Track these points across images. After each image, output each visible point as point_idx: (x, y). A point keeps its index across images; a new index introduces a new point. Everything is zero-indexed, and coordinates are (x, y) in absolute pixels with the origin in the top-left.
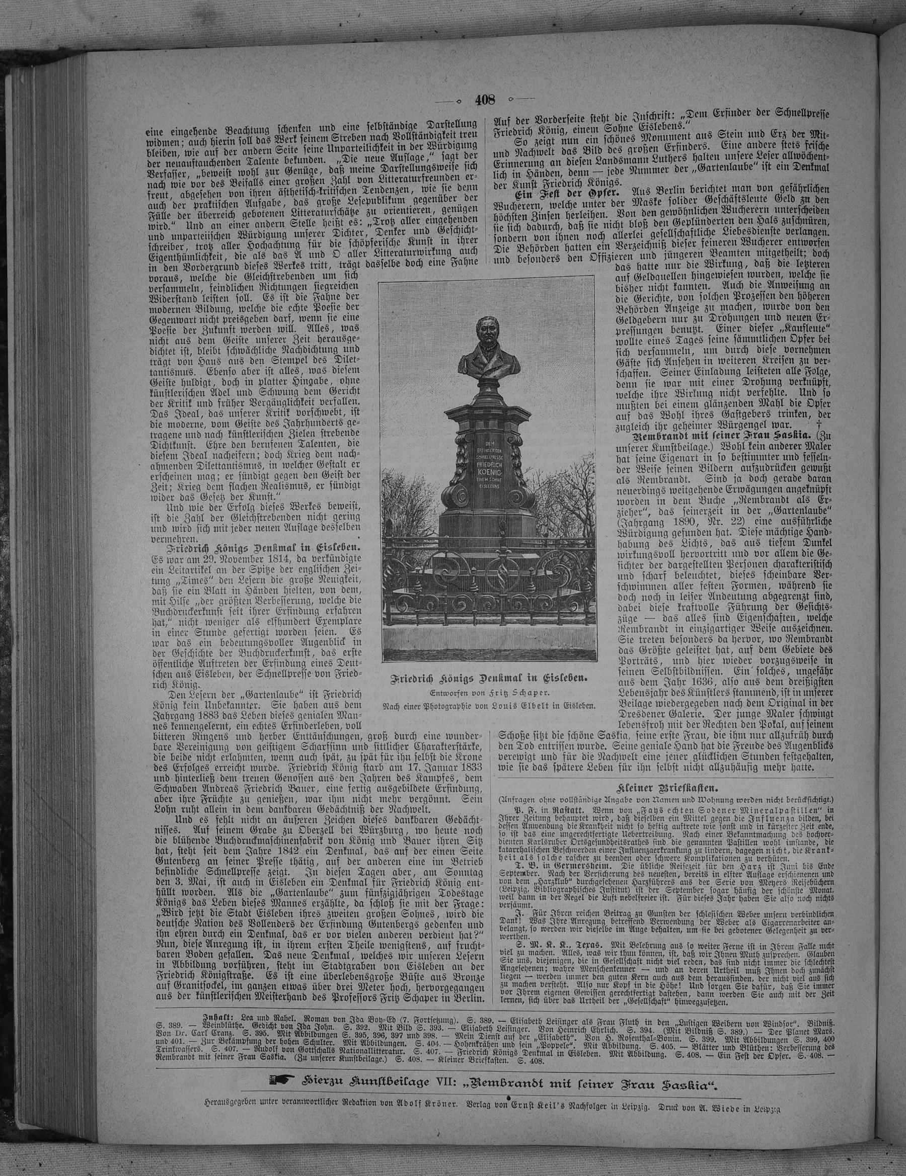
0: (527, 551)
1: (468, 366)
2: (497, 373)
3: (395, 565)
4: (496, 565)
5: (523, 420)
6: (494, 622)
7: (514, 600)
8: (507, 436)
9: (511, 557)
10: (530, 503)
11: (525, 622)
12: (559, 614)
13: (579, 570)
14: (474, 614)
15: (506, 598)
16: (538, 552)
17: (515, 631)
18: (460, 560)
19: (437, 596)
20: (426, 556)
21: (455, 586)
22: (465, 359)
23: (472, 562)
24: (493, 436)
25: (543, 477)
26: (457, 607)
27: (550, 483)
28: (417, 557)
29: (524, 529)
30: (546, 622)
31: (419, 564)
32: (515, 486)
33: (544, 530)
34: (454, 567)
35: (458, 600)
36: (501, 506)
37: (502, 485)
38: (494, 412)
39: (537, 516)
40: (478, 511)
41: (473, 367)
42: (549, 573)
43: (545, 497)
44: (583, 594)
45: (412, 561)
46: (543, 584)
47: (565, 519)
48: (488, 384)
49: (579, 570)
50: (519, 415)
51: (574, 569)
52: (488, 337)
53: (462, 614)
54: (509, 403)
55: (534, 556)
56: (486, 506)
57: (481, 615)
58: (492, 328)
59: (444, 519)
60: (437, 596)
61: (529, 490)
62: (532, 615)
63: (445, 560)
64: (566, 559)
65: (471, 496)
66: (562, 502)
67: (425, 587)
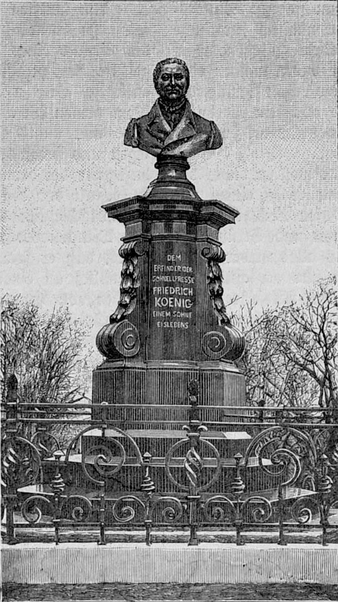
0: (231, 428)
1: (140, 134)
2: (185, 147)
3: (21, 447)
4: (183, 449)
5: (225, 222)
6: (179, 540)
7: (211, 505)
8: (200, 246)
9: (207, 437)
10: (237, 352)
11: (229, 540)
12: (282, 527)
13: (313, 459)
14: (147, 527)
15: (198, 502)
16: (248, 430)
17: (212, 554)
18: (124, 440)
19: (89, 498)
20: (72, 433)
21: (117, 481)
22: (135, 124)
23: (145, 444)
24: (178, 245)
25: (258, 313)
26: (121, 515)
27: (268, 321)
28: (56, 435)
29: (227, 393)
30: (261, 541)
31: (59, 447)
32: (213, 324)
33: (258, 395)
34: (116, 452)
35: (122, 504)
36: (190, 357)
37: (193, 323)
38: (180, 207)
39: (248, 373)
40: (155, 364)
41: (147, 138)
42: (266, 462)
43: (261, 343)
44: (320, 497)
45: (48, 442)
46: (256, 480)
47: (291, 379)
48: (171, 164)
49: (313, 459)
50: (219, 215)
51: (305, 457)
52: (172, 92)
53: (128, 526)
54: (205, 194)
55: (243, 435)
56: (167, 356)
57: (159, 527)
58: (178, 76)
59: (101, 377)
60: (89, 498)
61: (236, 331)
62: (239, 528)
63: (101, 440)
64: (293, 440)
65: (143, 340)
66: (286, 351)
67: (69, 484)
